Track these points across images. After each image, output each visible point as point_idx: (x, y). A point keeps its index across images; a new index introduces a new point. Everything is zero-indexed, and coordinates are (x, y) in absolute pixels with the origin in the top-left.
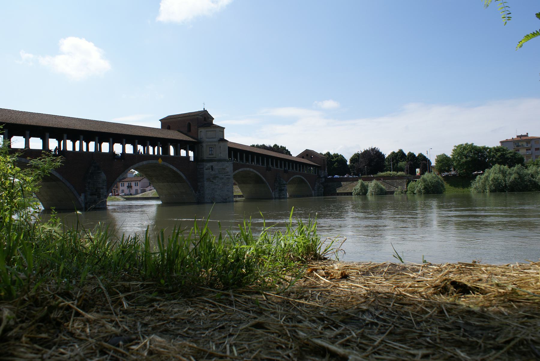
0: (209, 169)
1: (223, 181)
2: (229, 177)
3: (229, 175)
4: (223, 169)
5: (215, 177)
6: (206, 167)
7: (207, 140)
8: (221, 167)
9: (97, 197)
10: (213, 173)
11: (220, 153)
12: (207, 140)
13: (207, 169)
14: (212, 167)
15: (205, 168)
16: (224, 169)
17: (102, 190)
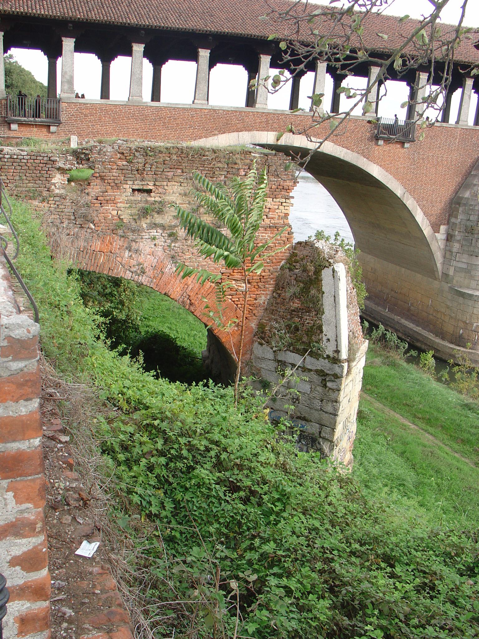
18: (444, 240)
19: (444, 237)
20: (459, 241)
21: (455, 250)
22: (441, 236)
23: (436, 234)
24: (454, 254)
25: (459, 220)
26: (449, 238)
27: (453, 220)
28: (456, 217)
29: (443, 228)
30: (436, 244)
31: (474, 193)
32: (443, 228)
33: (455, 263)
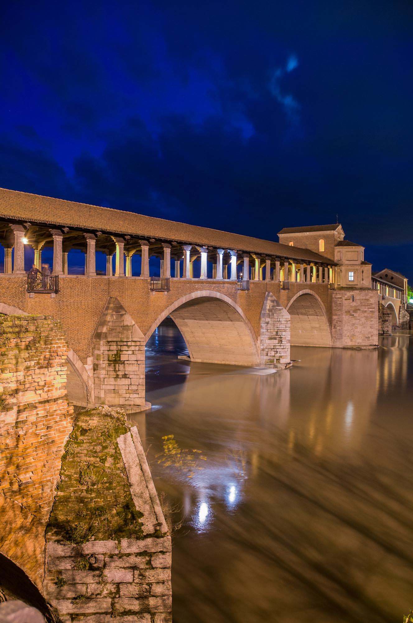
0: (349, 299)
1: (366, 314)
2: (374, 310)
3: (374, 308)
4: (366, 299)
5: (356, 311)
6: (346, 296)
7: (347, 262)
8: (364, 298)
9: (277, 341)
10: (354, 304)
11: (363, 280)
12: (347, 262)
13: (346, 300)
14: (353, 296)
15: (344, 298)
16: (368, 300)
17: (284, 333)
18: (92, 369)
19: (91, 366)
20: (103, 368)
21: (102, 376)
22: (89, 366)
23: (85, 366)
24: (102, 380)
25: (102, 351)
26: (96, 368)
27: (96, 352)
28: (99, 350)
29: (90, 360)
30: (87, 374)
31: (110, 328)
32: (90, 360)
33: (104, 387)
